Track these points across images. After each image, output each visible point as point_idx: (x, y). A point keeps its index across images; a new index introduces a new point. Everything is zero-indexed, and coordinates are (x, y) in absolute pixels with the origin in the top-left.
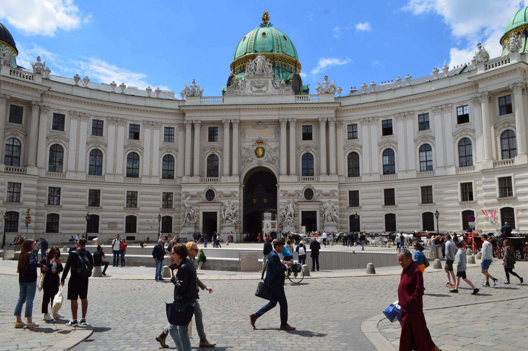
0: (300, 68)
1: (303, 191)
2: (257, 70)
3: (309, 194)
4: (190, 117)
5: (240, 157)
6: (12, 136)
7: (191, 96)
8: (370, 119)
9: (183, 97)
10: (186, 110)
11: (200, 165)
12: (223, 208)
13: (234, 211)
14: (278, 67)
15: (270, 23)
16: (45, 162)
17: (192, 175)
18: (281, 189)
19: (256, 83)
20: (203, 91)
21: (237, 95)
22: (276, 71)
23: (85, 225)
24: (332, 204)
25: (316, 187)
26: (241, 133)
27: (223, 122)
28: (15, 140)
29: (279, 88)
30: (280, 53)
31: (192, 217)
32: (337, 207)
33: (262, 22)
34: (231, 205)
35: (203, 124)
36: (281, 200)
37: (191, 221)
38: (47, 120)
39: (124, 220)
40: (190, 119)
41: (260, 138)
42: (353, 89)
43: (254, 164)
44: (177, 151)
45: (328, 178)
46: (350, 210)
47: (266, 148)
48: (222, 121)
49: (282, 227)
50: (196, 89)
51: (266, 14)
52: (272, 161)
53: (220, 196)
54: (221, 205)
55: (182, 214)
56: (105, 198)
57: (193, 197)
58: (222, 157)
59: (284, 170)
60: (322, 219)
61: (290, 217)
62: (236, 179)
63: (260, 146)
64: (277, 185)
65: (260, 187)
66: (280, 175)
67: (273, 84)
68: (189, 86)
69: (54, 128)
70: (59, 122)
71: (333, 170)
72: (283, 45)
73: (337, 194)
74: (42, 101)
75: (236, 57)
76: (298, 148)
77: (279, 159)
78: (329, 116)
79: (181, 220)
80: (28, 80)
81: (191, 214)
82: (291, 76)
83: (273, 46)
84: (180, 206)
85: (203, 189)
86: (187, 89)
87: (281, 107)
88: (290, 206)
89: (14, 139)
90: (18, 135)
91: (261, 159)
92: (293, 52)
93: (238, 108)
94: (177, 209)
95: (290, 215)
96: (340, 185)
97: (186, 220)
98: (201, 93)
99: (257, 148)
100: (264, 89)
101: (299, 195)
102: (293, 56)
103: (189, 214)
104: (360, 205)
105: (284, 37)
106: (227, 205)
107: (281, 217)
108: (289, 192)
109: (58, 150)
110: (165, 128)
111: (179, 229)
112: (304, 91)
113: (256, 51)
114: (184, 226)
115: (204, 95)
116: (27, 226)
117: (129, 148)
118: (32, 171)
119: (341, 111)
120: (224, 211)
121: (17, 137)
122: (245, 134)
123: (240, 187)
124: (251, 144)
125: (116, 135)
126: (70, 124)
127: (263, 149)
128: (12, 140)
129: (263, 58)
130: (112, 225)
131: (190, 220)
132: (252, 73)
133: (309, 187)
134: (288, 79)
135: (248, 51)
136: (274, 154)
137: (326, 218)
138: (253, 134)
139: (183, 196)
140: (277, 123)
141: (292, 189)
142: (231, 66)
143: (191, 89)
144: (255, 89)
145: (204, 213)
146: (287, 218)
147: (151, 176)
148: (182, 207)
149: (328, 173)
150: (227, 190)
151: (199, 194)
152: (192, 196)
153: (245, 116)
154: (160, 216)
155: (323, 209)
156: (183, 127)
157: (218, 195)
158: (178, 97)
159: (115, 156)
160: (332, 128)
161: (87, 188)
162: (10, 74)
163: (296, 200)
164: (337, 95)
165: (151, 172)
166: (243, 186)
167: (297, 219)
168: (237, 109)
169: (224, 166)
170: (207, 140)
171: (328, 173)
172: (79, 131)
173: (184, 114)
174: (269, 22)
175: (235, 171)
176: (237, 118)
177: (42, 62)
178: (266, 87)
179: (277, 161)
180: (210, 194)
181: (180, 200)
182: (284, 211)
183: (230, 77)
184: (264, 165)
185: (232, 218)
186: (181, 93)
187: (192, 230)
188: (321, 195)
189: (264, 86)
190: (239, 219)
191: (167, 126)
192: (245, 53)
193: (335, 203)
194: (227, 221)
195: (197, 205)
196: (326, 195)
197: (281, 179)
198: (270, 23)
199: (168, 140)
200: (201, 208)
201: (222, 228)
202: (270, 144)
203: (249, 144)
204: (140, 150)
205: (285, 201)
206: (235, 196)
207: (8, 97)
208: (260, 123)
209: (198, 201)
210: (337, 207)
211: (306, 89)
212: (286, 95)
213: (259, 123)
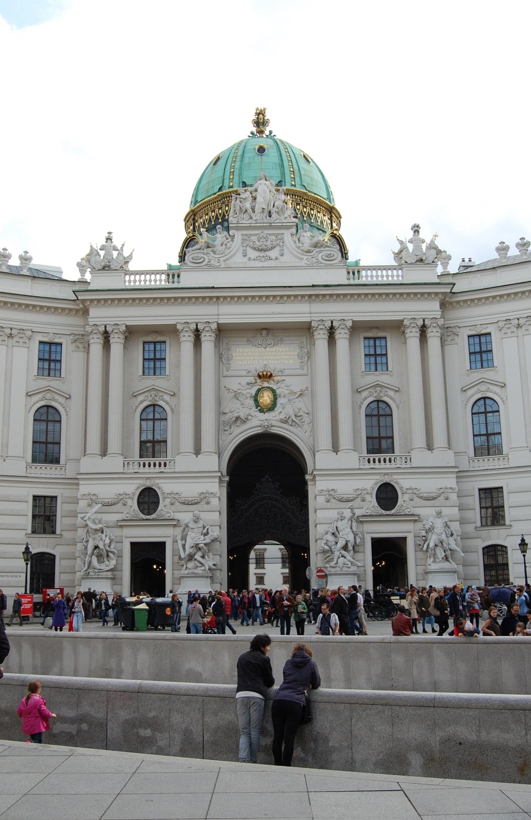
1: (373, 489)
4: (99, 316)
7: (103, 269)
9: (83, 272)
10: (92, 301)
11: (124, 430)
12: (178, 532)
13: (208, 540)
15: (271, 132)
19: (254, 238)
20: (130, 257)
21: (210, 267)
24: (446, 519)
26: (221, 357)
27: (179, 327)
30: (298, 188)
31: (105, 554)
32: (455, 527)
33: (254, 130)
34: (201, 524)
35: (131, 333)
37: (103, 567)
42: (467, 263)
44: (69, 398)
46: (484, 532)
48: (175, 325)
50: (115, 254)
51: (260, 113)
54: (175, 526)
55: (80, 546)
60: (421, 555)
61: (344, 552)
63: (266, 384)
64: (307, 477)
65: (267, 482)
68: (97, 246)
72: (302, 172)
73: (453, 497)
75: (199, 199)
79: (79, 561)
81: (101, 546)
83: (283, 174)
84: (74, 528)
85: (132, 488)
86: (93, 253)
91: (268, 415)
94: (66, 535)
95: (345, 548)
96: (461, 475)
97: (90, 562)
98: (127, 262)
99: (259, 390)
100: (273, 254)
102: (325, 197)
103: (96, 547)
104: (507, 522)
105: (304, 156)
106: (191, 525)
107: (324, 552)
108: (339, 492)
110: (40, 342)
119: (451, 303)
120: (184, 538)
122: (229, 359)
123: (221, 481)
127: (273, 391)
131: (99, 562)
133: (388, 481)
135: (226, 184)
136: (302, 405)
138: (249, 357)
140: (305, 329)
141: (345, 487)
142: (186, 220)
143: (102, 253)
144: (253, 254)
145: (133, 545)
146: (337, 554)
150: (190, 489)
155: (424, 533)
157: (168, 501)
158: (72, 273)
160: (434, 342)
163: (358, 512)
166: (227, 479)
167: (359, 556)
168: (211, 298)
169: (179, 430)
170: (141, 373)
173: (85, 312)
178: (277, 249)
180: (148, 500)
182: (331, 538)
184: (275, 430)
185: (203, 557)
186: (79, 265)
188: (416, 499)
189: (272, 248)
191: (46, 340)
192: (220, 189)
194: (191, 565)
198: (271, 132)
199: (46, 372)
200: (127, 532)
201: (178, 580)
202: (289, 380)
203: (240, 383)
205: (333, 514)
206: (208, 503)
208: (264, 333)
209: (119, 517)
210: (455, 527)
212: (327, 267)
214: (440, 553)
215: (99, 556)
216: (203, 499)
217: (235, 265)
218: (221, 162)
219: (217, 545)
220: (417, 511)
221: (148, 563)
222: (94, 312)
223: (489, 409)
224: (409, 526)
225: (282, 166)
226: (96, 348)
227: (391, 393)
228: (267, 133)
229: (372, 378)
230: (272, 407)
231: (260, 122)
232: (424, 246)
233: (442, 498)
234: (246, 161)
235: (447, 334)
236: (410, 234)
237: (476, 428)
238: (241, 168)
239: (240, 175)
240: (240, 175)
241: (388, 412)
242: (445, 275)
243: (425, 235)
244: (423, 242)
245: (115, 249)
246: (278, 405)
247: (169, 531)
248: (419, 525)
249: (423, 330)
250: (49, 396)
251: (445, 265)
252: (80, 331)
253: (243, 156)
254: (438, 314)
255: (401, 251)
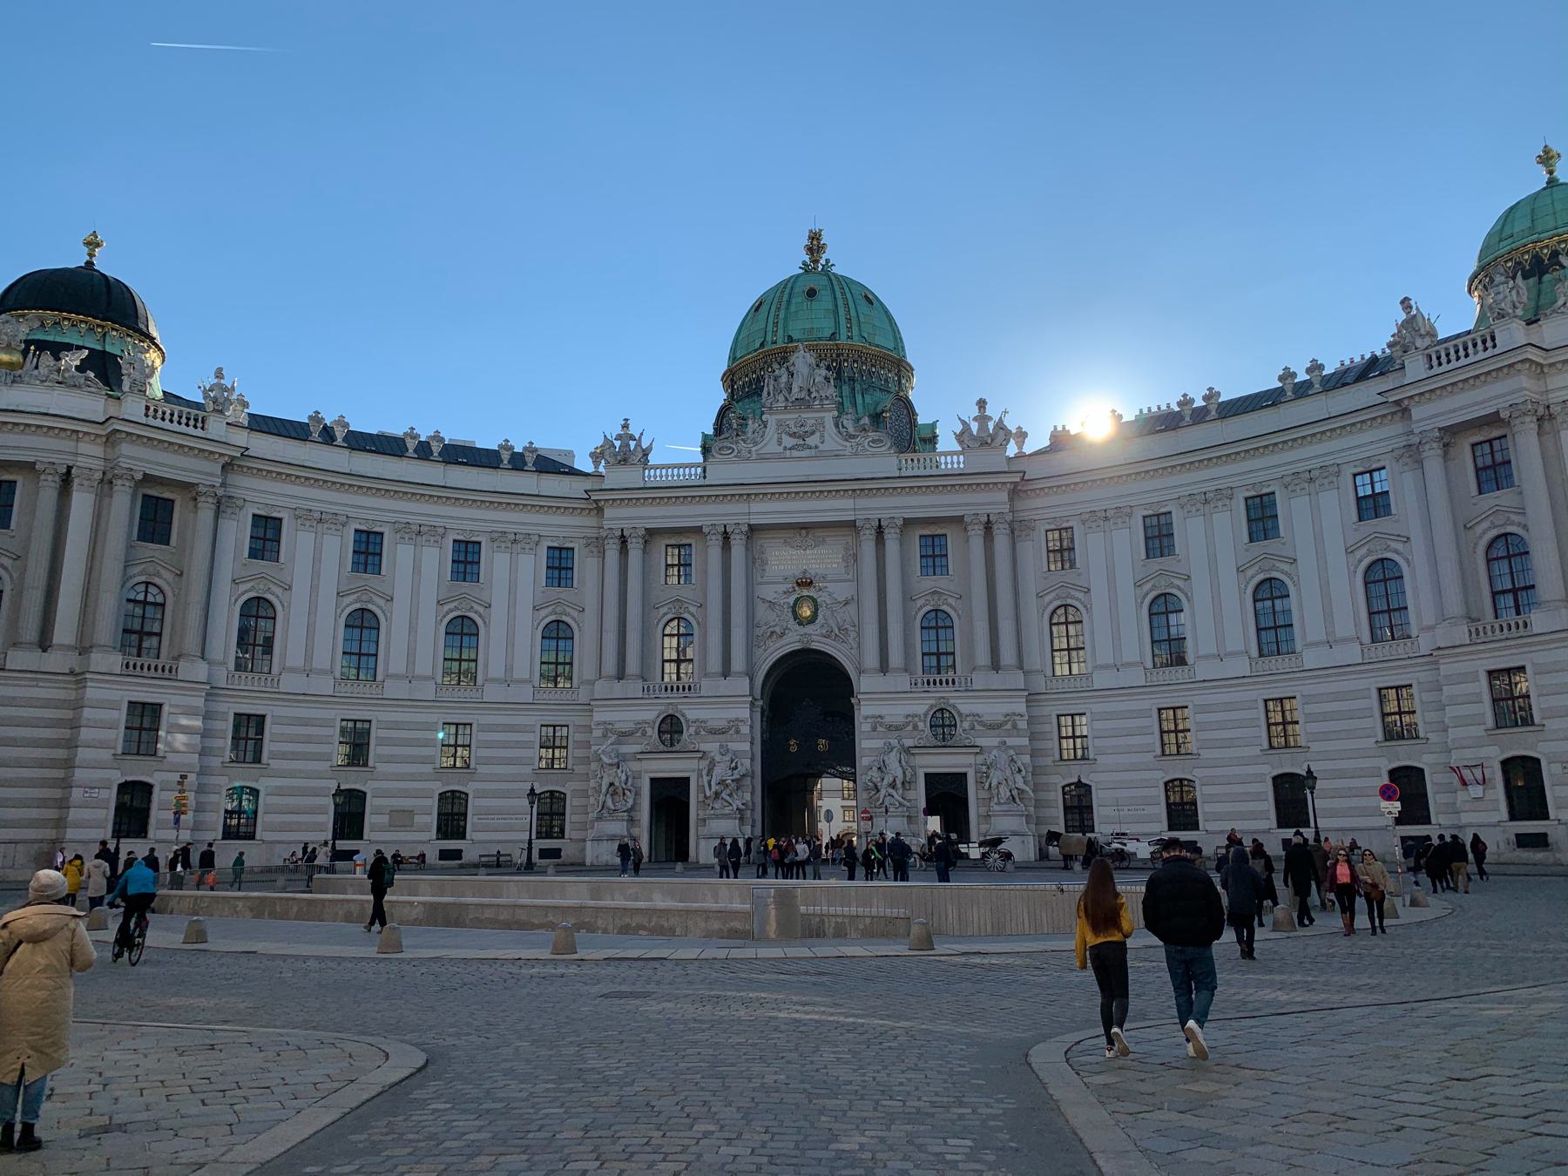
0: (909, 380)
1: (926, 715)
2: (795, 389)
3: (943, 725)
4: (616, 518)
5: (751, 623)
6: (143, 578)
8: (1110, 514)
9: (596, 464)
12: (704, 764)
14: (852, 379)
15: (827, 261)
16: (227, 646)
17: (621, 675)
18: (865, 711)
20: (650, 448)
22: (846, 389)
23: (328, 819)
25: (965, 706)
28: (152, 589)
29: (854, 437)
30: (857, 342)
31: (620, 791)
33: (807, 258)
36: (867, 744)
38: (237, 533)
39: (434, 803)
40: (617, 525)
41: (805, 572)
43: (791, 641)
45: (995, 680)
47: (822, 598)
49: (871, 818)
50: (632, 444)
51: (815, 237)
52: (839, 633)
53: (697, 733)
55: (592, 783)
56: (382, 742)
57: (624, 736)
58: (703, 625)
59: (871, 659)
62: (742, 686)
63: (805, 593)
64: (853, 700)
65: (807, 707)
66: (860, 672)
67: (837, 426)
69: (254, 554)
70: (266, 536)
71: (1008, 655)
73: (1023, 725)
74: (223, 485)
76: (908, 597)
77: (858, 626)
78: (993, 510)
80: (191, 430)
82: (887, 401)
83: (837, 323)
85: (651, 714)
86: (608, 443)
87: (859, 487)
88: (892, 760)
89: (147, 583)
90: (158, 575)
91: (809, 629)
92: (891, 337)
93: (744, 492)
94: (579, 769)
95: (893, 785)
100: (811, 441)
101: (915, 727)
103: (612, 784)
106: (718, 758)
108: (887, 720)
109: (262, 613)
111: (584, 826)
112: (923, 440)
113: (791, 339)
114: (599, 819)
115: (653, 459)
116: (177, 821)
117: (452, 606)
118: (195, 670)
120: (710, 773)
121: (157, 580)
122: (764, 563)
124: (783, 587)
125: (416, 570)
126: (297, 542)
127: (814, 600)
128: (142, 588)
129: (811, 358)
130: (402, 818)
132: (781, 398)
134: (879, 409)
135: (769, 339)
137: (994, 792)
138: (784, 560)
139: (597, 733)
141: (895, 712)
143: (617, 443)
144: (789, 441)
145: (653, 780)
146: (883, 792)
147: (508, 682)
148: (594, 766)
149: (996, 666)
150: (716, 716)
151: (637, 731)
152: (623, 734)
153: (764, 512)
154: (532, 790)
155: (984, 769)
156: (597, 544)
157: (692, 730)
159: (412, 629)
161: (336, 715)
162: (147, 415)
163: (908, 743)
164: (1012, 450)
165: (509, 668)
171: (996, 666)
172: (317, 560)
174: (824, 256)
175: (738, 663)
176: (744, 520)
177: (227, 382)
178: (818, 434)
179: (853, 635)
181: (588, 745)
182: (875, 774)
183: (722, 408)
184: (814, 646)
185: (730, 795)
187: (618, 827)
189: (813, 433)
190: (751, 795)
192: (762, 345)
193: (1019, 750)
195: (637, 757)
196: (993, 727)
197: (865, 684)
198: (827, 261)
200: (645, 765)
201: (703, 821)
202: (831, 587)
203: (773, 591)
204: (481, 609)
205: (878, 744)
206: (738, 732)
207: (139, 476)
209: (638, 748)
211: (926, 434)
213: (804, 529)
214: (1004, 792)
215: (615, 793)
216: (734, 725)
217: (768, 457)
218: (764, 308)
219: (748, 781)
220: (979, 741)
221: (670, 801)
222: (608, 512)
223: (1071, 618)
224: (971, 759)
225: (836, 312)
226: (612, 554)
227: (951, 601)
228: (823, 262)
229: (930, 583)
230: (812, 620)
231: (815, 246)
232: (991, 425)
233: (1009, 726)
234: (793, 309)
235: (1016, 529)
236: (975, 412)
237: (1056, 641)
238: (786, 318)
239: (785, 327)
240: (785, 327)
241: (948, 623)
242: (1020, 456)
243: (993, 411)
244: (990, 418)
245: (632, 438)
246: (820, 616)
247: (694, 764)
248: (980, 759)
249: (988, 527)
250: (559, 609)
251: (1020, 445)
252: (592, 533)
253: (789, 302)
254: (1006, 508)
255: (962, 433)
